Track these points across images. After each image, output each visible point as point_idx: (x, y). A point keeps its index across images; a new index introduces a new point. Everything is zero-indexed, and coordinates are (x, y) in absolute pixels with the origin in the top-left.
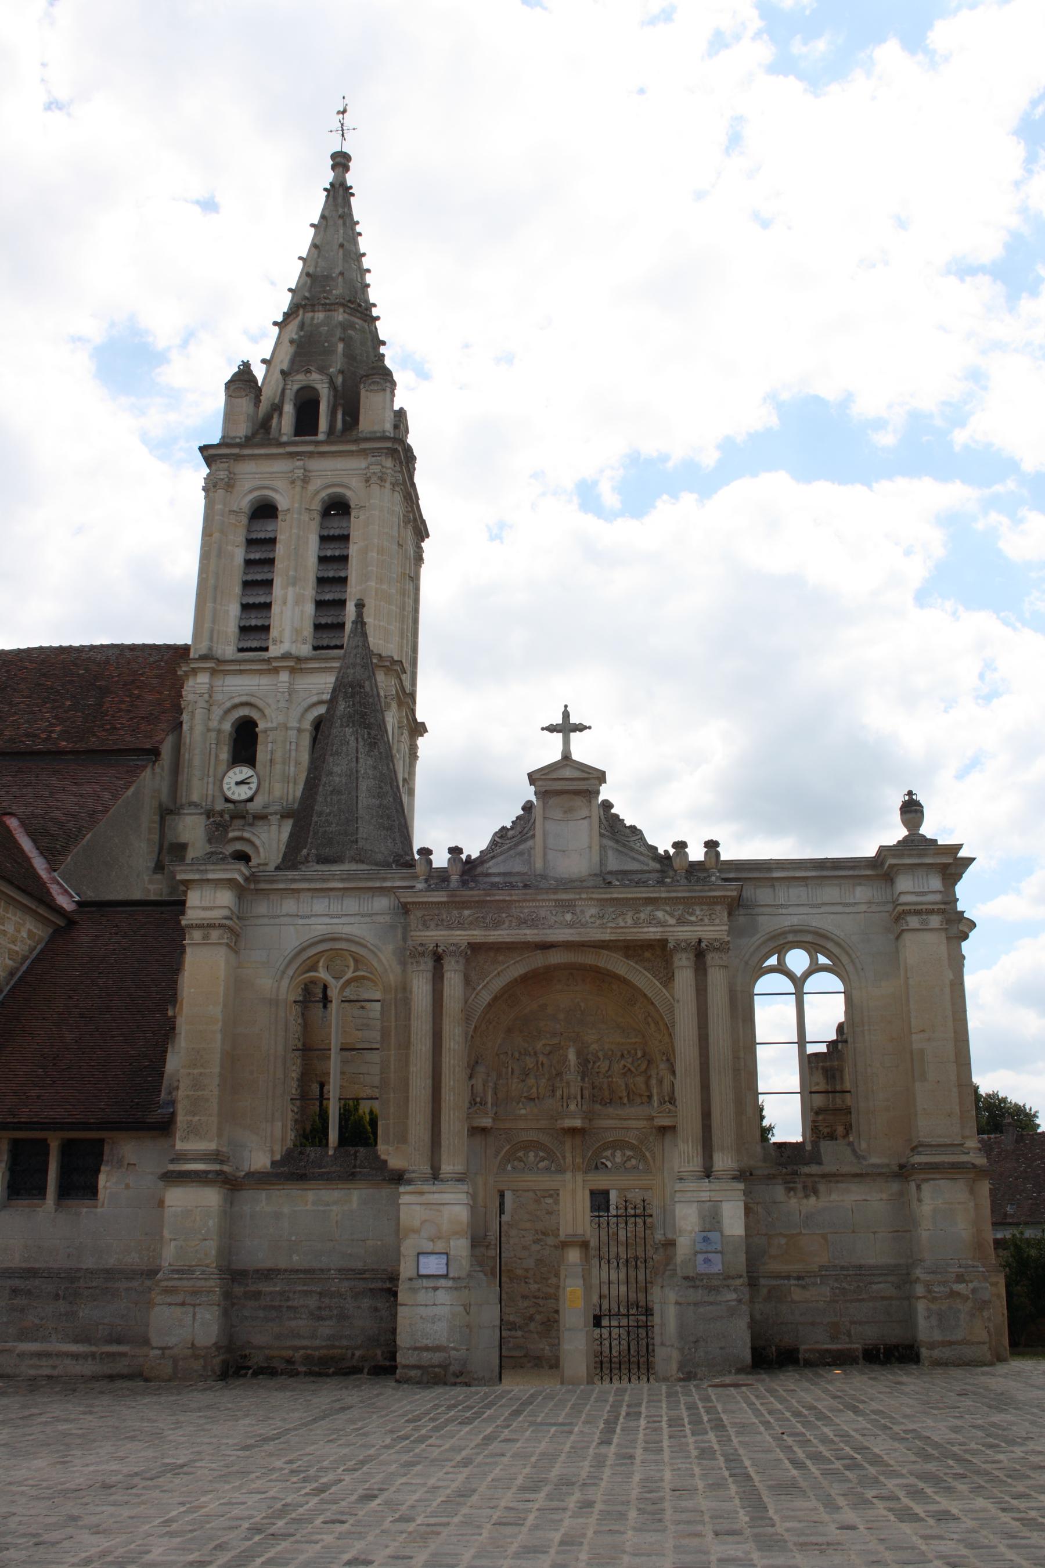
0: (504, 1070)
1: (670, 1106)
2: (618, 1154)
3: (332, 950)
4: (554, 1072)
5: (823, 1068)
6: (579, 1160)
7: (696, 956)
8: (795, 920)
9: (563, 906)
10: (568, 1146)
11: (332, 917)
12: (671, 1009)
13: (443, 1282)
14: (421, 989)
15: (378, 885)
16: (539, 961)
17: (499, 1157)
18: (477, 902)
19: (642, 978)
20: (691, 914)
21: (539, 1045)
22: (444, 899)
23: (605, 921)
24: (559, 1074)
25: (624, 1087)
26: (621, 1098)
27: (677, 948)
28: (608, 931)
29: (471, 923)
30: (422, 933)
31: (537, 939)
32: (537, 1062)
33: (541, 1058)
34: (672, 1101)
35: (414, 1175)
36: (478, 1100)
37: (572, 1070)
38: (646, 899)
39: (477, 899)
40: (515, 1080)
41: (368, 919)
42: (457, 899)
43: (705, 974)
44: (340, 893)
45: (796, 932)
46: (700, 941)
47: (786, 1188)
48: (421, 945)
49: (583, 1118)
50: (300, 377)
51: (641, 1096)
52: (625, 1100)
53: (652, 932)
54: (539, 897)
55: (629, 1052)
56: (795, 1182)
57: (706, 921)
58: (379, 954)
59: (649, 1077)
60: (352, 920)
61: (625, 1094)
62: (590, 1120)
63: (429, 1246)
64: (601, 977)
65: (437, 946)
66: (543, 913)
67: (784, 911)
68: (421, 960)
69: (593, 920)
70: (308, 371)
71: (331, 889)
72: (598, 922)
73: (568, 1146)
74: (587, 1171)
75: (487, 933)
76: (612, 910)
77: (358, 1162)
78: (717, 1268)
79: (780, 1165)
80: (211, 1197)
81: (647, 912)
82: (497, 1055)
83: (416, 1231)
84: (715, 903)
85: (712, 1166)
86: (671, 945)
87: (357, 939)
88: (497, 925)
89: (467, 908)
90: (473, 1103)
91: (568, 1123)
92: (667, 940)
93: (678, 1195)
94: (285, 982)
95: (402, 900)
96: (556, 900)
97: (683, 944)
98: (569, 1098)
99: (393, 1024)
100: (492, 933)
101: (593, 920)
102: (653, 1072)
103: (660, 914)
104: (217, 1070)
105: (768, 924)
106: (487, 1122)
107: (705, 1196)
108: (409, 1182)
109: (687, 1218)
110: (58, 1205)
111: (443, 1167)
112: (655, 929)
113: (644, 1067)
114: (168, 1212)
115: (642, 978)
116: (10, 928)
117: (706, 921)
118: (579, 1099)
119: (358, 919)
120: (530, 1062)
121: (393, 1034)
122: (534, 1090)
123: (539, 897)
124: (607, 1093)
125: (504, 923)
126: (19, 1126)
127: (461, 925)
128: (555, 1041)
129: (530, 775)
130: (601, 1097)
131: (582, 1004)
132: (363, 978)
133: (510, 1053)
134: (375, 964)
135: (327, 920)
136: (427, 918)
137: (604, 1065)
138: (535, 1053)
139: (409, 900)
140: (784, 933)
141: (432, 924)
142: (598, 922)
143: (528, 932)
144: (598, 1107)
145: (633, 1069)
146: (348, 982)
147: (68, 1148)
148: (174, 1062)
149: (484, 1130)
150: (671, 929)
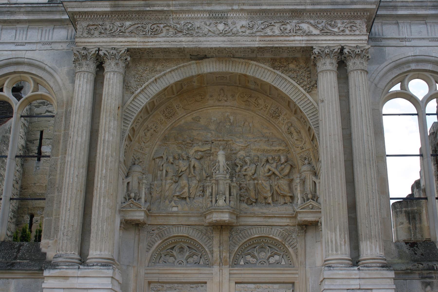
0: (159, 173)
1: (313, 203)
4: (205, 175)
5: (406, 212)
6: (225, 254)
7: (338, 63)
8: (417, 51)
9: (216, 18)
10: (216, 242)
11: (17, 44)
12: (315, 112)
14: (83, 87)
15: (57, 17)
17: (151, 252)
18: (138, 12)
19: (287, 85)
20: (333, 26)
21: (192, 152)
22: (108, 9)
23: (255, 30)
24: (210, 176)
25: (268, 188)
26: (265, 198)
27: (323, 54)
28: (258, 39)
29: (131, 32)
30: (86, 40)
31: (191, 45)
32: (190, 165)
33: (193, 162)
34: (315, 198)
35: (60, 259)
36: (132, 195)
37: (221, 169)
38: (293, 11)
39: (138, 9)
40: (169, 181)
41: (48, 47)
42: (120, 9)
43: (347, 78)
44: (25, 26)
45: (418, 61)
46: (342, 49)
47: (423, 283)
48: (85, 49)
49: (231, 213)
51: (284, 196)
52: (270, 200)
53: (298, 41)
54: (194, 8)
55: (273, 159)
56: (431, 278)
57: (347, 32)
58: (55, 75)
59: (291, 181)
60: (34, 47)
61: (269, 194)
62: (237, 217)
64: (250, 91)
65: (99, 50)
66: (197, 24)
67: (408, 44)
68: (84, 62)
69: (243, 30)
71: (18, 22)
72: (248, 32)
73: (216, 242)
75: (146, 40)
76: (260, 22)
77: (20, 254)
79: (415, 261)
81: (294, 24)
82: (154, 159)
84: (356, 17)
85: (359, 256)
86: (316, 51)
87: (37, 63)
88: (155, 33)
89: (127, 19)
90: (128, 198)
91: (216, 217)
92: (312, 47)
93: (327, 282)
95: (69, 10)
96: (210, 12)
97: (326, 50)
98: (217, 194)
99: (63, 132)
100: (150, 40)
101: (243, 30)
103: (305, 26)
105: (394, 54)
108: (53, 266)
111: (91, 252)
112: (300, 38)
113: (287, 171)
115: (287, 85)
117: (347, 32)
118: (228, 196)
119: (39, 46)
120: (183, 165)
121: (61, 141)
122: (186, 189)
123: (194, 8)
124: (252, 194)
125: (161, 32)
127: (122, 33)
128: (207, 147)
130: (247, 197)
131: (232, 118)
134: (51, 84)
135: (13, 47)
136: (91, 27)
138: (188, 158)
139: (76, 10)
140: (408, 62)
141: (96, 33)
142: (248, 32)
143: (183, 39)
144: (244, 205)
145: (277, 173)
150: (316, 38)
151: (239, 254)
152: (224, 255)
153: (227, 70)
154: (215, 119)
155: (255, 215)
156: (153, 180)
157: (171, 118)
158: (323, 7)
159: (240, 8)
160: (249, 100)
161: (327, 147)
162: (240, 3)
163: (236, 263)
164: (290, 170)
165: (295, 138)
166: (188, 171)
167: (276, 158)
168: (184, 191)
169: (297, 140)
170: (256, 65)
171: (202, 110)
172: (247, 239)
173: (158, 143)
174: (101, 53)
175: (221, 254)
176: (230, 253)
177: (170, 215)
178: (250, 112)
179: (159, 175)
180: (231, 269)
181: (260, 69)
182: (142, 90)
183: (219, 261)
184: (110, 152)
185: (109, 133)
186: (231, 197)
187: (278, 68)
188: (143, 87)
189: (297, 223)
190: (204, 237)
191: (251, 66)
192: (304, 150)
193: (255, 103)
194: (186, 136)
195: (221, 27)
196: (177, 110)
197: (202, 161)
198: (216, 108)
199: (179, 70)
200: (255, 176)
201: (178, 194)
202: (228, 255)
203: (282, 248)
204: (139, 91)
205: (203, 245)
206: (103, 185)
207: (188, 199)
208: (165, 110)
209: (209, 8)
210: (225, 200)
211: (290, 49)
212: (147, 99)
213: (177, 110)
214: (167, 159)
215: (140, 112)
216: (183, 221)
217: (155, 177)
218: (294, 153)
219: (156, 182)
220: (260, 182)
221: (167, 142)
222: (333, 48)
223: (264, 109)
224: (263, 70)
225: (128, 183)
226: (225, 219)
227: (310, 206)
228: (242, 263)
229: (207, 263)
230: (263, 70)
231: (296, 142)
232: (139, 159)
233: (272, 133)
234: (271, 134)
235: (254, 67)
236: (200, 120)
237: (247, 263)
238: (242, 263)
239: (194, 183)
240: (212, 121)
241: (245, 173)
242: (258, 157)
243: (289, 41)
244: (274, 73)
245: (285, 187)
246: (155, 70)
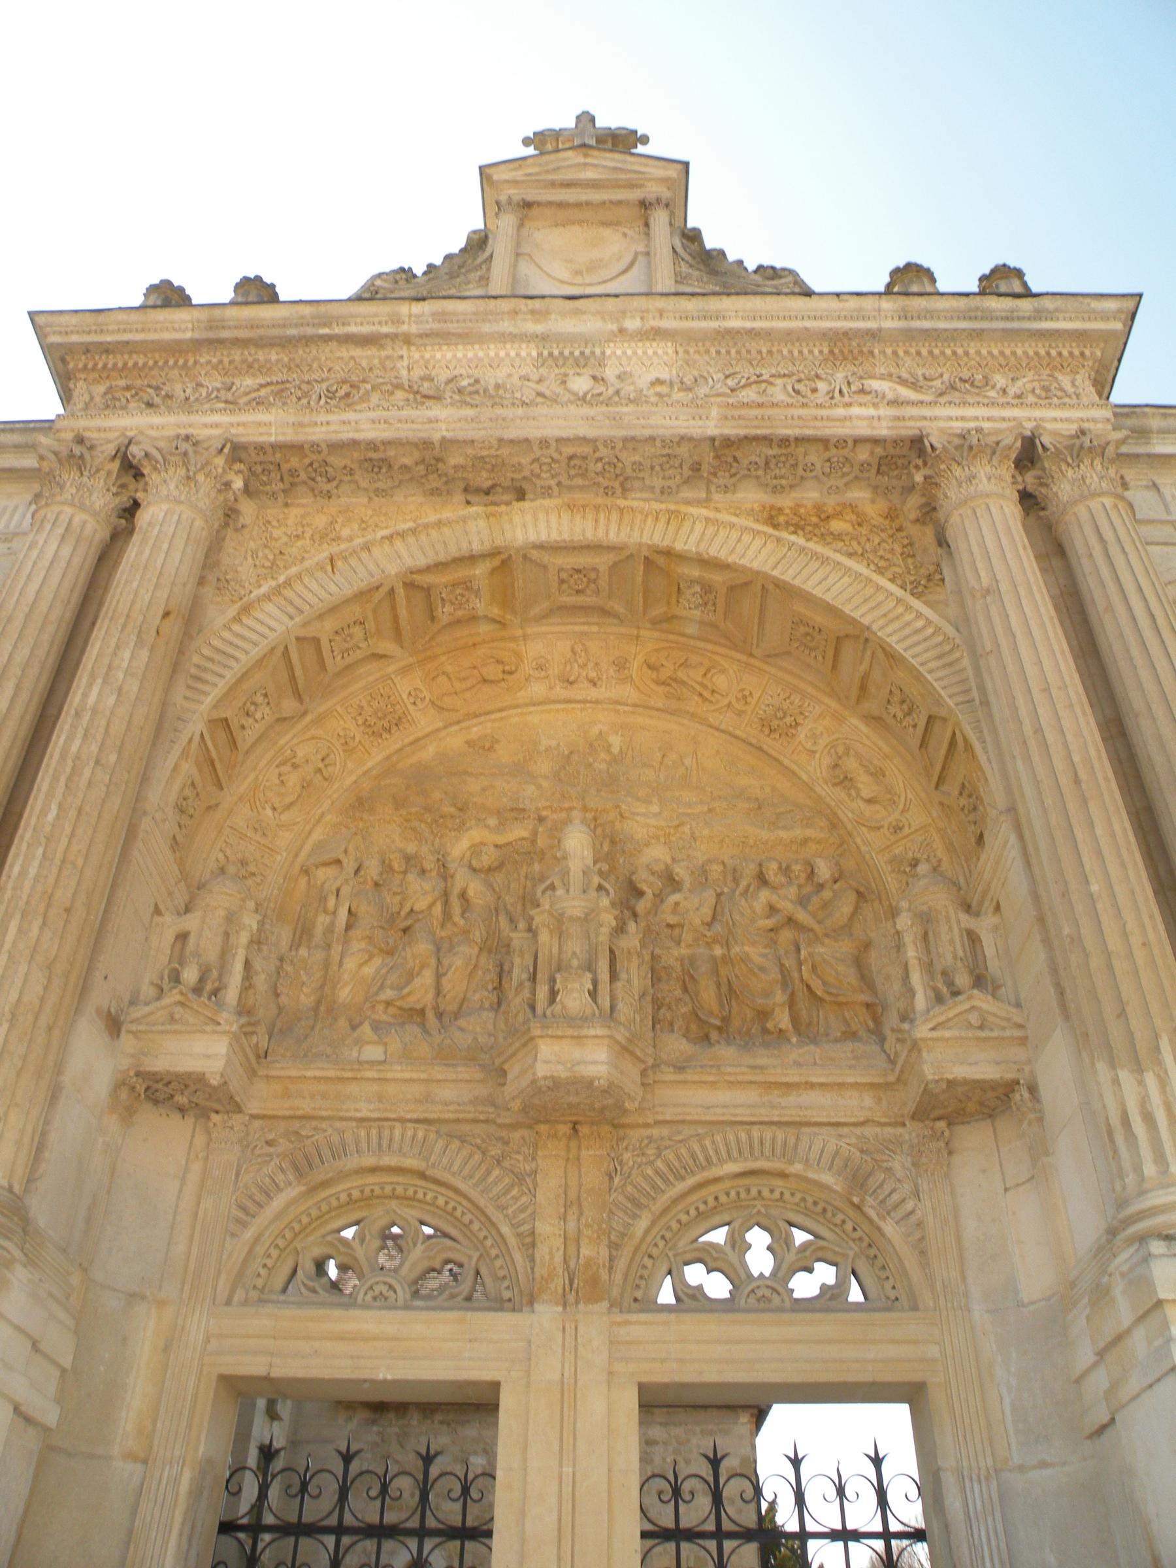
2: (758, 1238)
16: (472, 528)
21: (459, 847)
26: (763, 1015)
32: (446, 895)
52: (783, 1020)
72: (678, 396)
82: (305, 871)
84: (1056, 364)
96: (544, 338)
100: (322, 417)
118: (604, 975)
120: (421, 893)
128: (519, 832)
129: (481, 168)
131: (616, 742)
133: (350, 865)
145: (802, 916)
151: (655, 1252)
152: (586, 1251)
153: (601, 533)
154: (553, 743)
156: (295, 945)
157: (385, 735)
158: (942, 325)
159: (647, 326)
160: (681, 675)
161: (1039, 730)
162: (648, 311)
163: (639, 1294)
164: (857, 908)
165: (866, 793)
166: (438, 909)
167: (797, 868)
168: (417, 982)
169: (870, 801)
170: (707, 520)
171: (504, 714)
172: (691, 1181)
173: (328, 818)
174: (134, 449)
175: (572, 1250)
176: (613, 1246)
178: (685, 721)
179: (319, 929)
180: (619, 1318)
181: (723, 533)
182: (277, 590)
183: (559, 1282)
184: (94, 748)
185: (105, 682)
186: (619, 984)
187: (792, 529)
188: (282, 579)
189: (911, 1107)
190: (496, 1172)
191: (687, 524)
192: (906, 831)
193: (702, 684)
194: (437, 795)
195: (581, 384)
196: (411, 708)
197: (499, 879)
198: (558, 711)
199: (423, 537)
200: (718, 927)
201: (388, 994)
202: (604, 1252)
203: (849, 1226)
204: (264, 589)
205: (491, 1210)
206: (32, 871)
207: (430, 1015)
208: (364, 704)
209: (540, 328)
210: (593, 994)
211: (834, 451)
212: (291, 618)
213: (411, 708)
214: (357, 871)
215: (259, 663)
217: (303, 934)
218: (863, 848)
219: (303, 952)
220: (736, 950)
221: (365, 816)
222: (995, 438)
223: (739, 706)
224: (735, 535)
225: (183, 937)
226: (590, 1071)
227: (974, 1018)
228: (666, 1296)
229: (507, 1294)
230: (735, 535)
231: (868, 810)
232: (244, 863)
233: (774, 788)
234: (768, 790)
235: (699, 527)
236: (497, 746)
237: (690, 1298)
238: (666, 1296)
240: (542, 748)
241: (672, 919)
242: (723, 863)
243: (829, 419)
244: (778, 540)
245: (841, 968)
246: (333, 535)
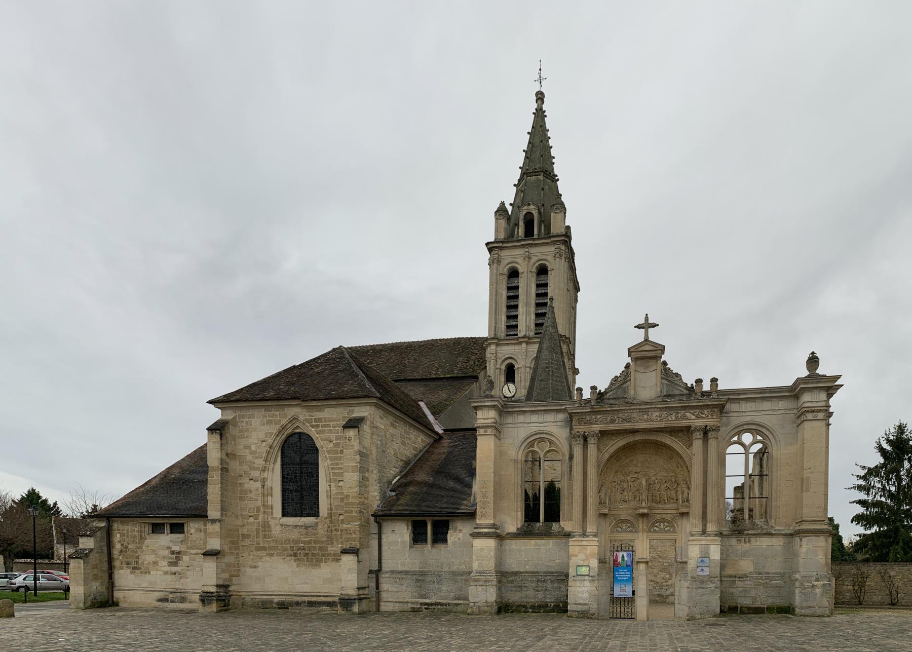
3: (540, 438)
13: (587, 578)
21: (629, 478)
34: (688, 501)
50: (526, 207)
63: (581, 563)
70: (529, 205)
74: (649, 531)
78: (707, 572)
80: (491, 543)
83: (576, 556)
91: (641, 511)
94: (521, 452)
102: (679, 489)
104: (492, 489)
106: (606, 511)
107: (703, 542)
109: (694, 552)
110: (432, 546)
114: (474, 549)
116: (412, 437)
120: (625, 485)
124: (658, 499)
126: (416, 515)
130: (655, 500)
132: (553, 450)
137: (657, 486)
146: (548, 452)
147: (435, 525)
148: (476, 488)
149: (605, 515)
155: (658, 508)
177: (619, 509)
216: (625, 512)
217: (612, 492)
239: (631, 494)
